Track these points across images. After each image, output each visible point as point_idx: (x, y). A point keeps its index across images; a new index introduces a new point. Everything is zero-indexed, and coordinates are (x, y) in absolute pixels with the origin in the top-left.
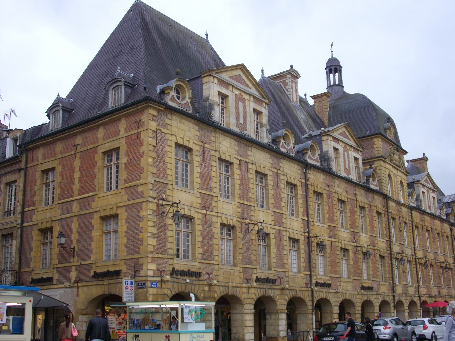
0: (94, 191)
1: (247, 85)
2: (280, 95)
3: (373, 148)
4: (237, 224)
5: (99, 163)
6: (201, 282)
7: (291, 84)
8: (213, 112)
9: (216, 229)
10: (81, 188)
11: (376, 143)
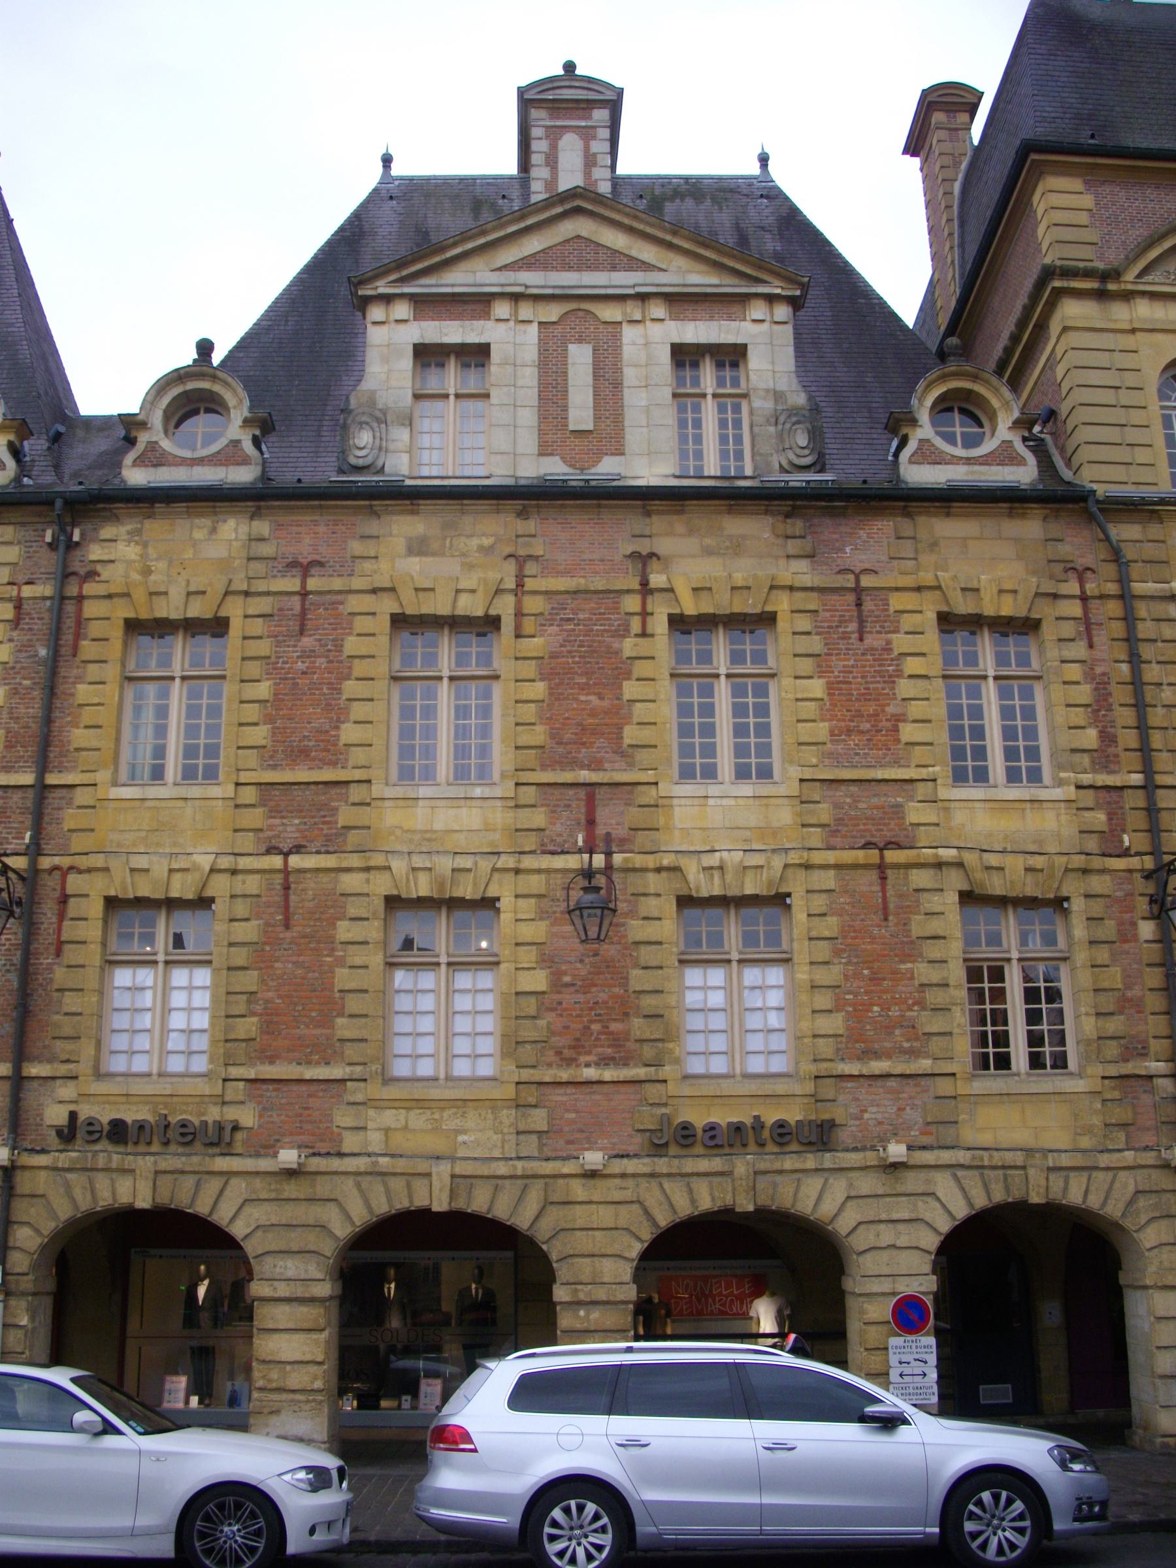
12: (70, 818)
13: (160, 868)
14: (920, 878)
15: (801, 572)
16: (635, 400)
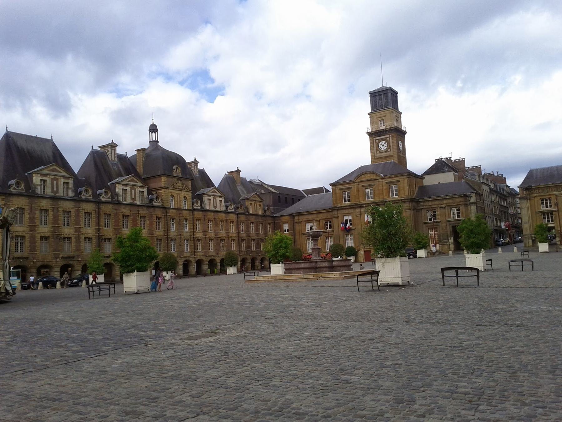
4: (50, 235)
6: (29, 261)
9: (38, 239)
12: (101, 231)
13: (108, 235)
14: (154, 237)
15: (147, 212)
16: (137, 195)
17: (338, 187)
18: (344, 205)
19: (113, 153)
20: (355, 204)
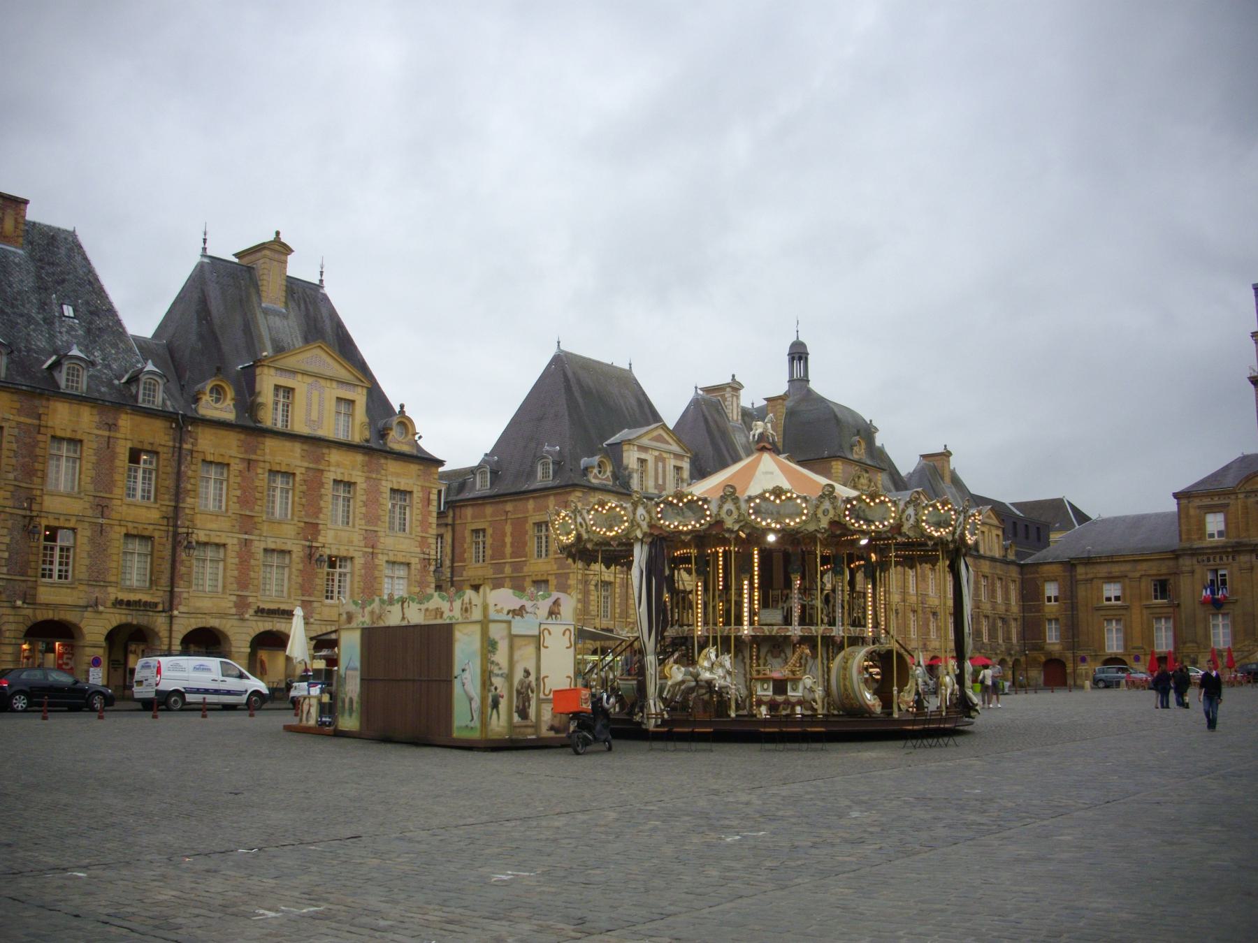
0: (526, 556)
1: (668, 443)
2: (716, 416)
3: (830, 471)
5: (530, 532)
7: (730, 399)
8: (631, 481)
10: (513, 552)
11: (834, 467)
17: (1197, 502)
18: (1209, 545)
19: (735, 405)
20: (1236, 542)
